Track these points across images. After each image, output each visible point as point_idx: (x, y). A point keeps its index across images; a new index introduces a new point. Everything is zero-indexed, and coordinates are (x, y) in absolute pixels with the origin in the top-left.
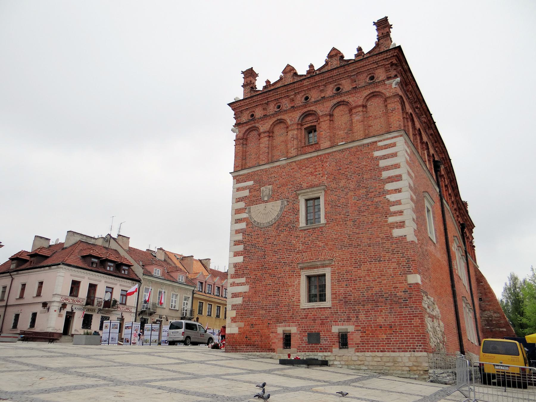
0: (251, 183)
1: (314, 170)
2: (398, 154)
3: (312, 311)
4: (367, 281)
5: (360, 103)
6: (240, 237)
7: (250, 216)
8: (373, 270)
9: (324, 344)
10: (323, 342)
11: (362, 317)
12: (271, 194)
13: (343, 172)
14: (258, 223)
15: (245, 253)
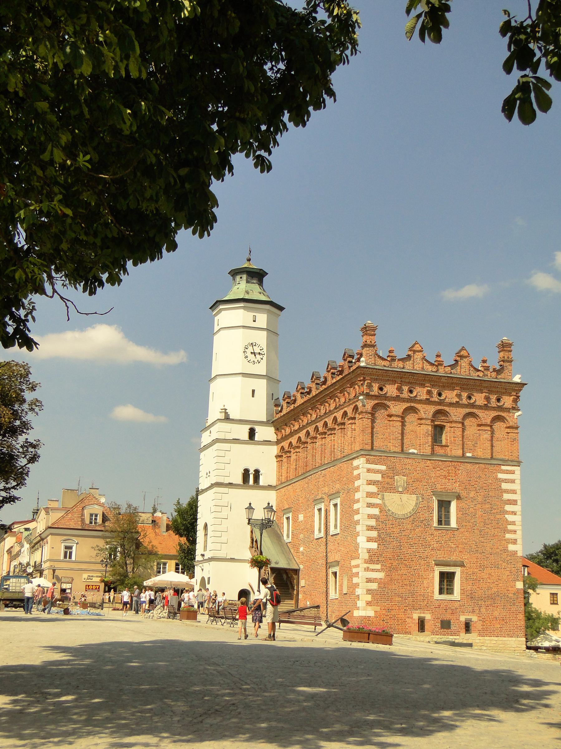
0: (383, 468)
1: (447, 475)
2: (516, 481)
3: (445, 602)
4: (488, 583)
5: (489, 423)
6: (373, 523)
7: (384, 503)
8: (493, 574)
9: (454, 630)
10: (452, 627)
11: (483, 610)
12: (405, 486)
13: (472, 484)
14: (393, 513)
15: (379, 540)
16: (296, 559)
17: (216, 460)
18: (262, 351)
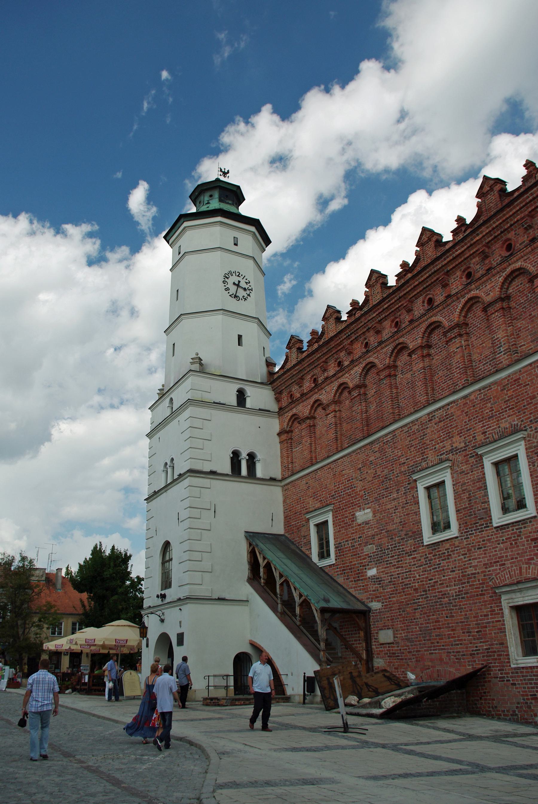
16: (354, 593)
17: (187, 434)
18: (249, 285)
